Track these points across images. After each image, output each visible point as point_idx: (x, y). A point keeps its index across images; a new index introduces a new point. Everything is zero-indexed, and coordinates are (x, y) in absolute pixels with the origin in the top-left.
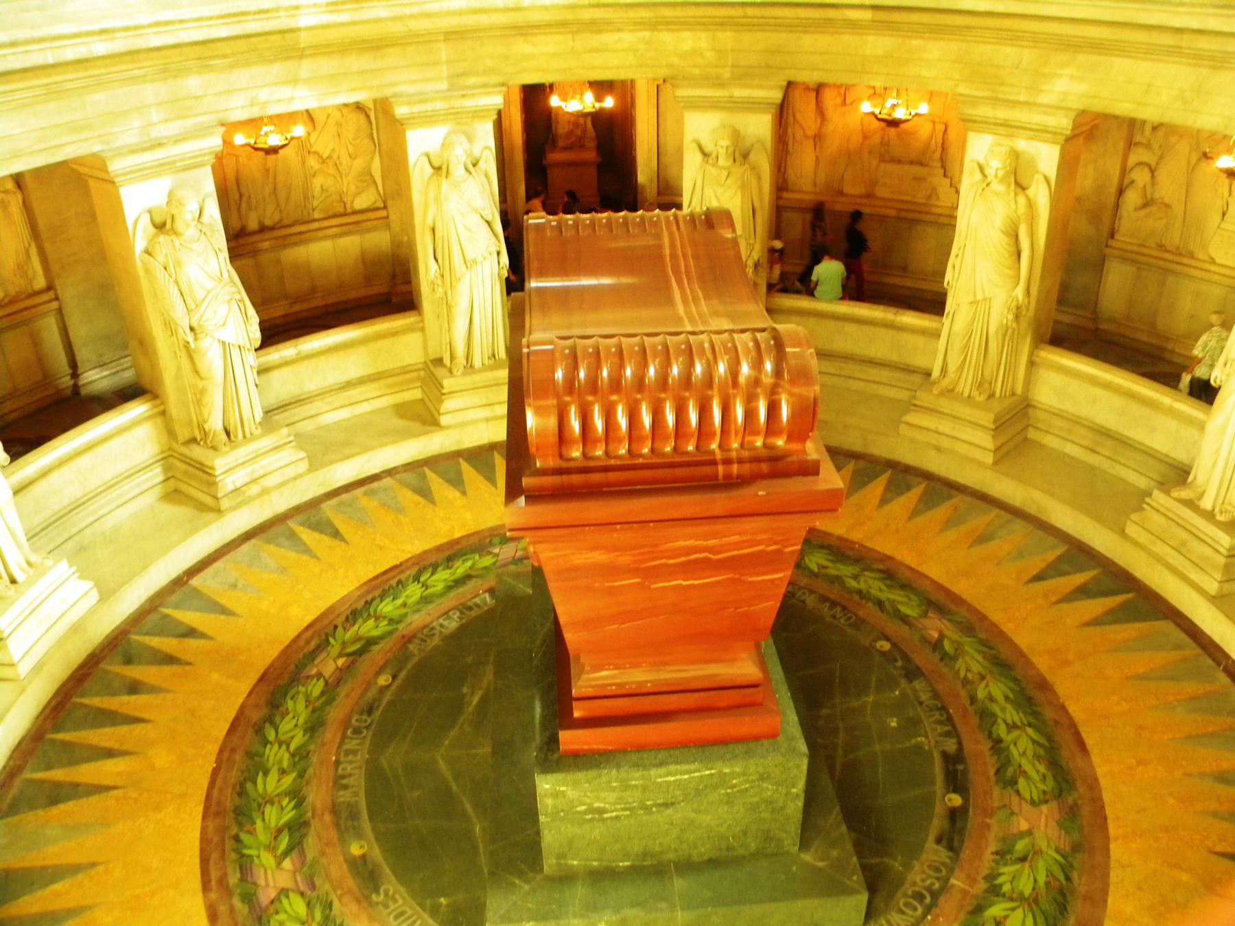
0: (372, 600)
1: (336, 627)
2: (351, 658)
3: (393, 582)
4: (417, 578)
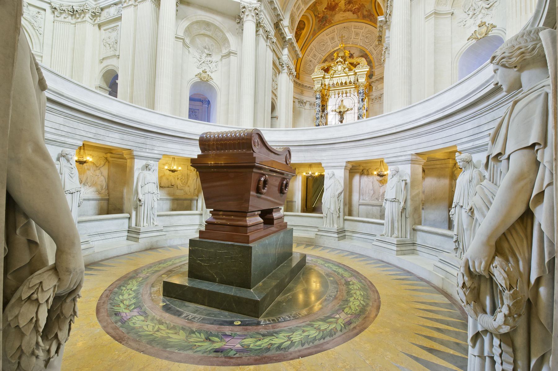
0: (320, 339)
1: (341, 331)
2: (333, 316)
3: (306, 346)
4: (293, 343)
